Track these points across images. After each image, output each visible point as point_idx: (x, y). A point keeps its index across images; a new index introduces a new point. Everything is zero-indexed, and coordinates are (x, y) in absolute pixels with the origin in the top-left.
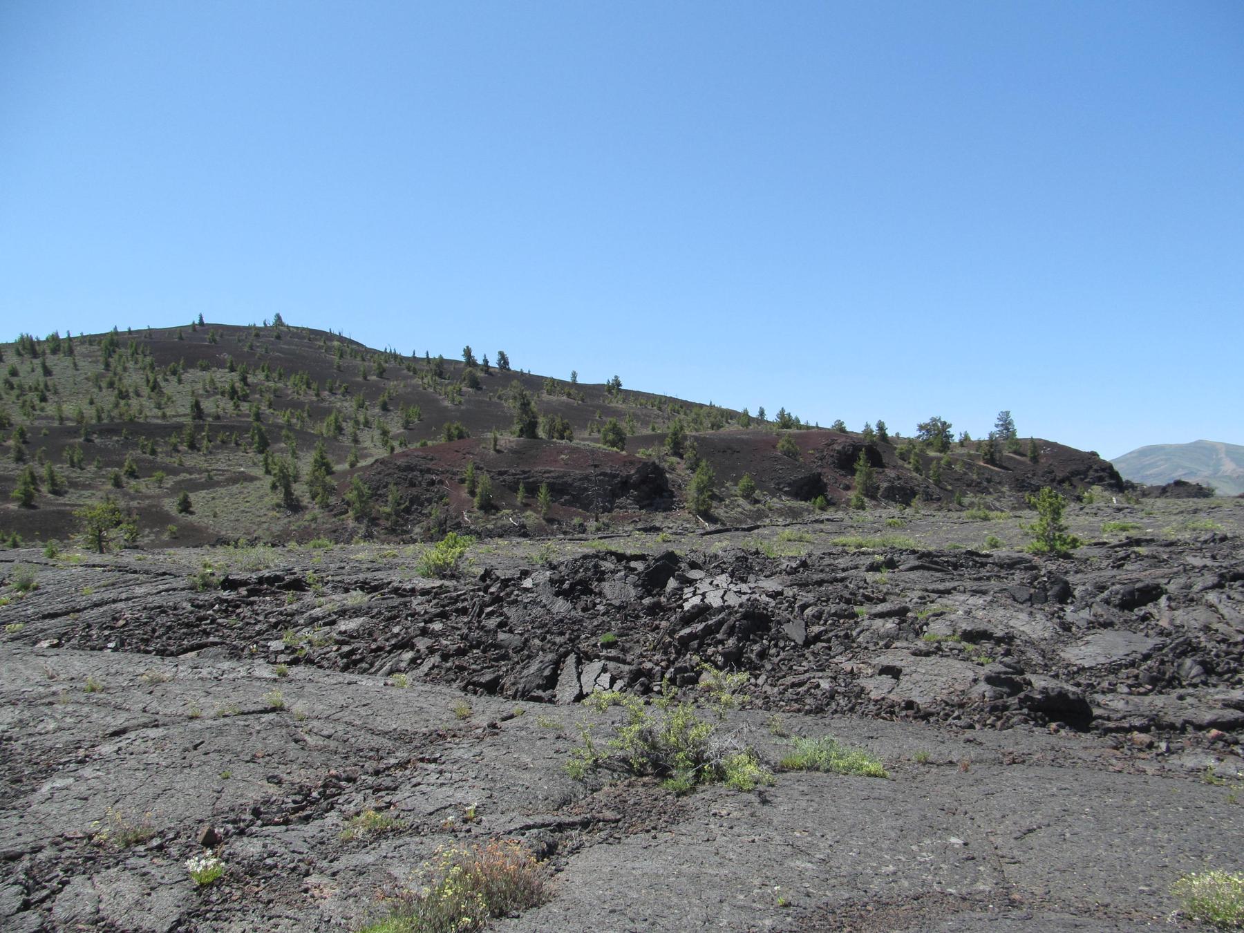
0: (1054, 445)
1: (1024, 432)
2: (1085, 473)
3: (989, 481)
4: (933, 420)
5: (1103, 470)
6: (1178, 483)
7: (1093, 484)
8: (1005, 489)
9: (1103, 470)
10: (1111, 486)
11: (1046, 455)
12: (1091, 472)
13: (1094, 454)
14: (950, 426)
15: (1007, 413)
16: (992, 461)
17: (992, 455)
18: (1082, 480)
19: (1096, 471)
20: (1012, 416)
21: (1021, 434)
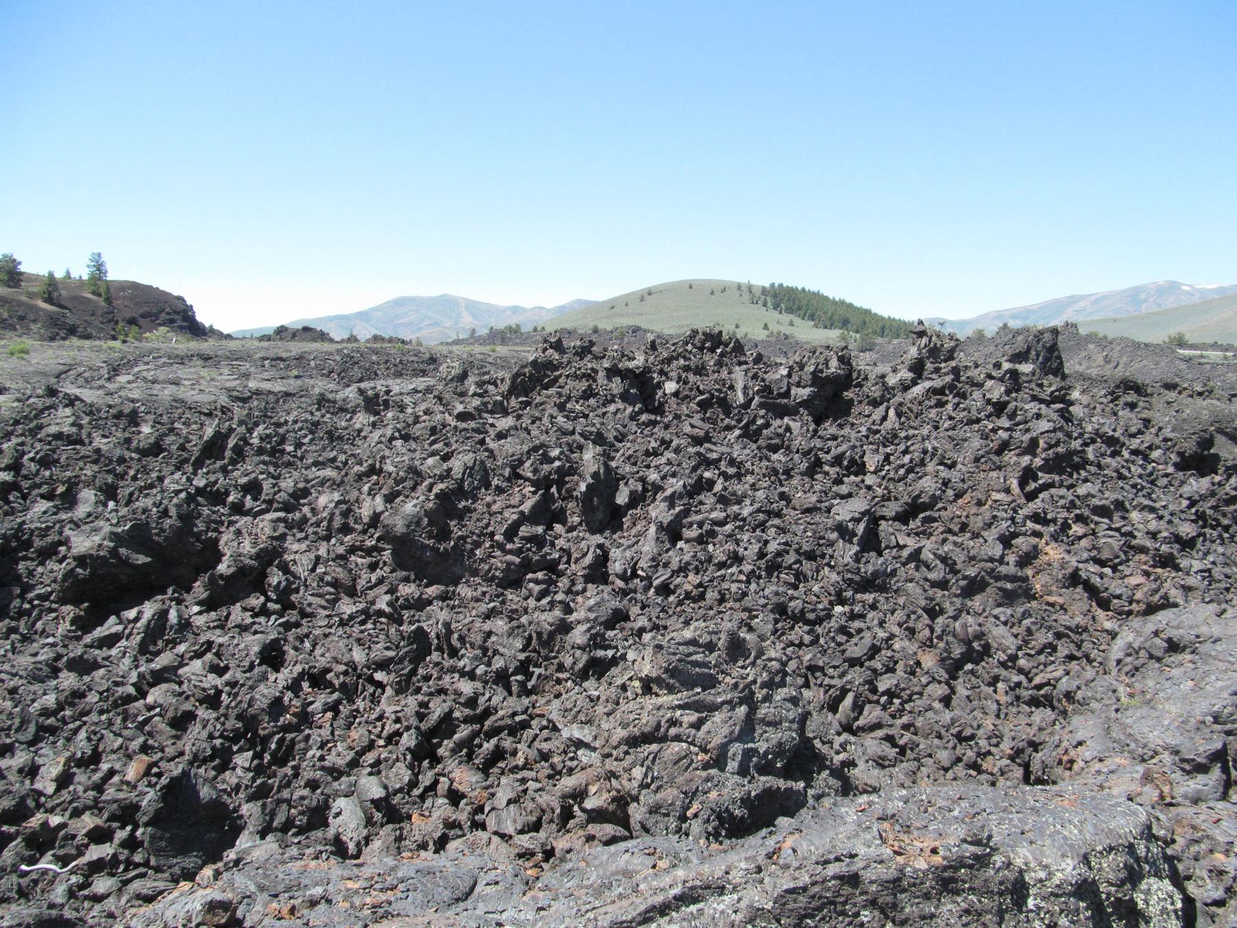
0: (135, 286)
1: (116, 273)
2: (157, 316)
3: (22, 318)
4: (5, 256)
5: (176, 313)
6: (306, 329)
7: (160, 325)
8: (35, 327)
9: (176, 313)
10: (181, 328)
11: (124, 297)
12: (163, 315)
13: (181, 299)
14: (20, 263)
15: (99, 255)
16: (49, 300)
17: (50, 293)
18: (153, 321)
19: (168, 314)
20: (104, 258)
21: (111, 276)
